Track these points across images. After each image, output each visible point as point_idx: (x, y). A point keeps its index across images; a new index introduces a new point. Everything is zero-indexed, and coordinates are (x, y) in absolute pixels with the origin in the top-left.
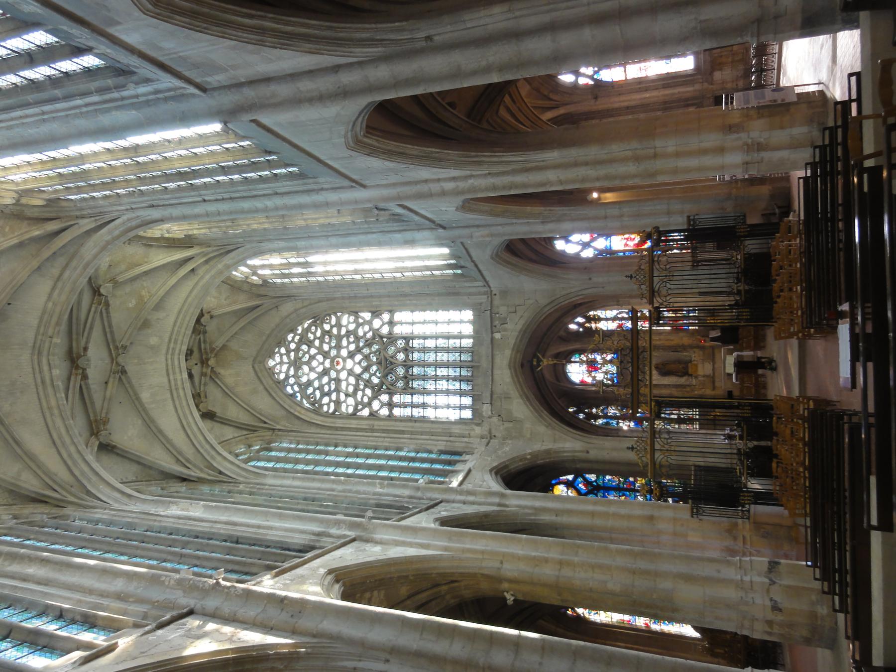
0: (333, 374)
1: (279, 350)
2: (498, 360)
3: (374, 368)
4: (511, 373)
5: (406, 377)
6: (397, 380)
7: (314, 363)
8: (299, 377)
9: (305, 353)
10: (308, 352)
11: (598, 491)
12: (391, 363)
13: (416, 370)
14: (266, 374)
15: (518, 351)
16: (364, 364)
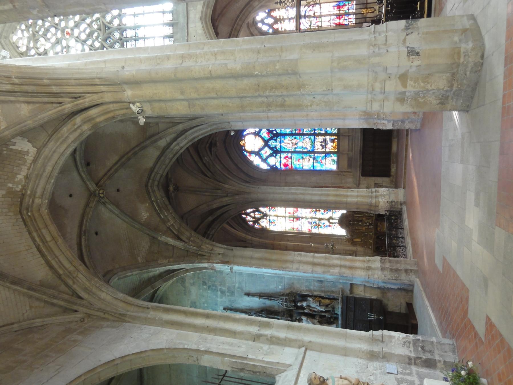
0: (64, 43)
1: (20, 27)
2: (192, 15)
3: (96, 34)
4: (203, 25)
5: (121, 39)
6: (115, 42)
7: (49, 35)
8: (38, 48)
9: (40, 27)
10: (43, 25)
11: (277, 137)
12: (109, 28)
13: (130, 33)
14: (11, 47)
15: (208, 7)
16: (88, 31)
